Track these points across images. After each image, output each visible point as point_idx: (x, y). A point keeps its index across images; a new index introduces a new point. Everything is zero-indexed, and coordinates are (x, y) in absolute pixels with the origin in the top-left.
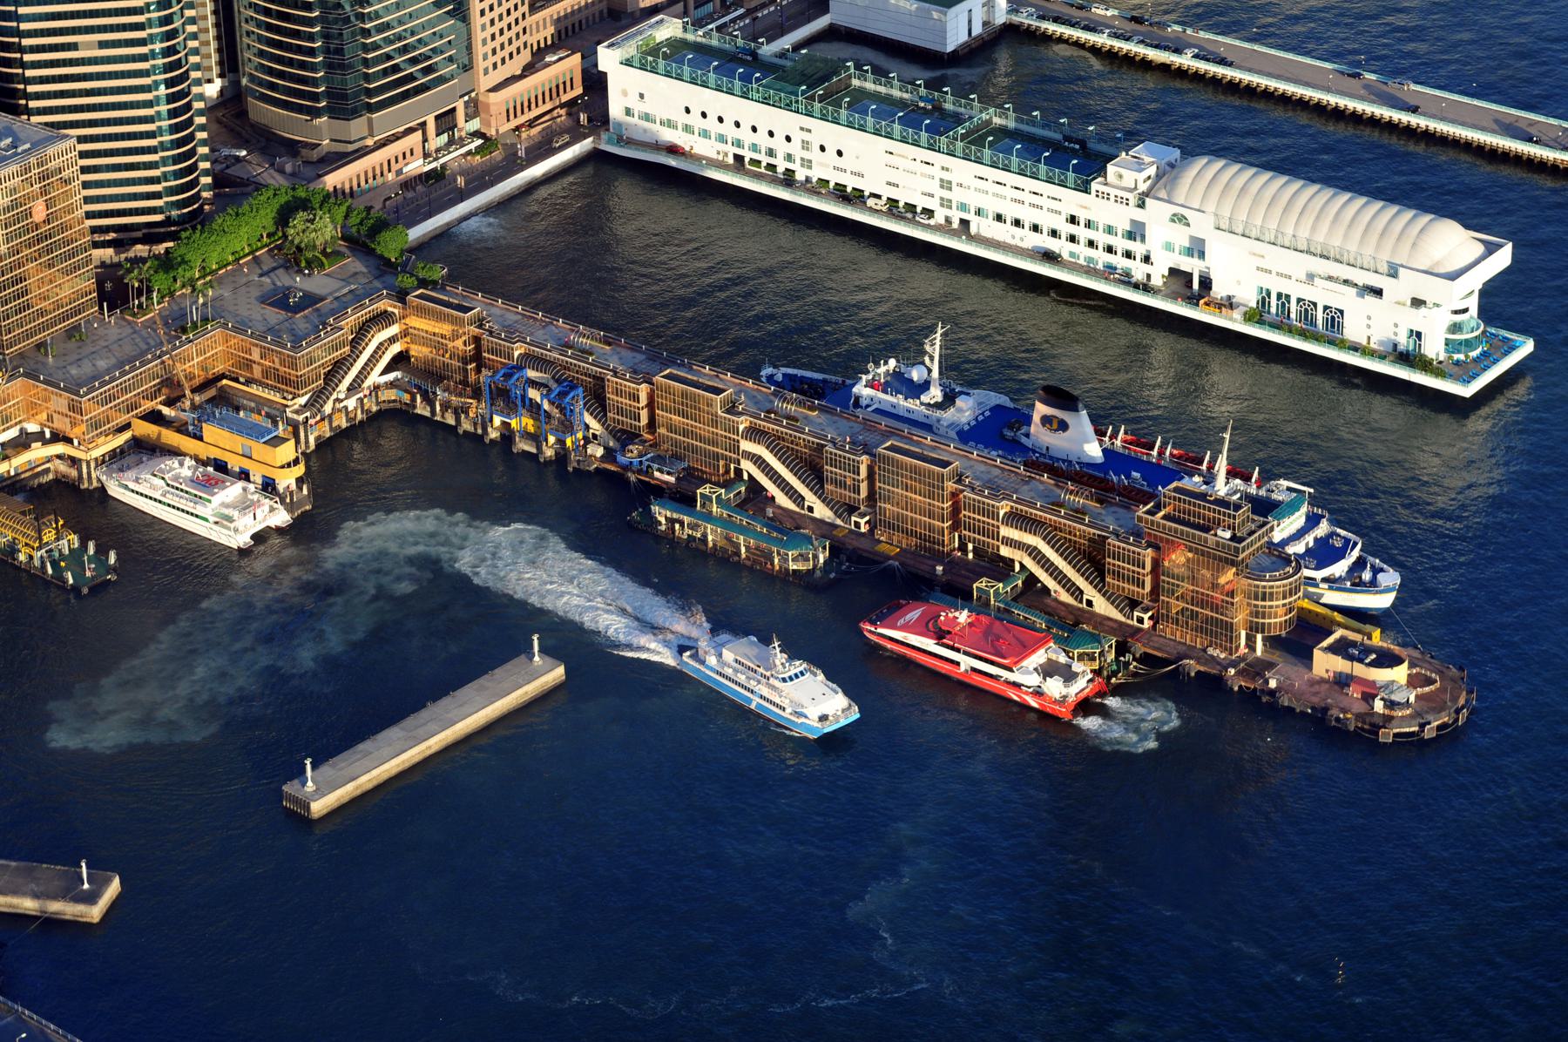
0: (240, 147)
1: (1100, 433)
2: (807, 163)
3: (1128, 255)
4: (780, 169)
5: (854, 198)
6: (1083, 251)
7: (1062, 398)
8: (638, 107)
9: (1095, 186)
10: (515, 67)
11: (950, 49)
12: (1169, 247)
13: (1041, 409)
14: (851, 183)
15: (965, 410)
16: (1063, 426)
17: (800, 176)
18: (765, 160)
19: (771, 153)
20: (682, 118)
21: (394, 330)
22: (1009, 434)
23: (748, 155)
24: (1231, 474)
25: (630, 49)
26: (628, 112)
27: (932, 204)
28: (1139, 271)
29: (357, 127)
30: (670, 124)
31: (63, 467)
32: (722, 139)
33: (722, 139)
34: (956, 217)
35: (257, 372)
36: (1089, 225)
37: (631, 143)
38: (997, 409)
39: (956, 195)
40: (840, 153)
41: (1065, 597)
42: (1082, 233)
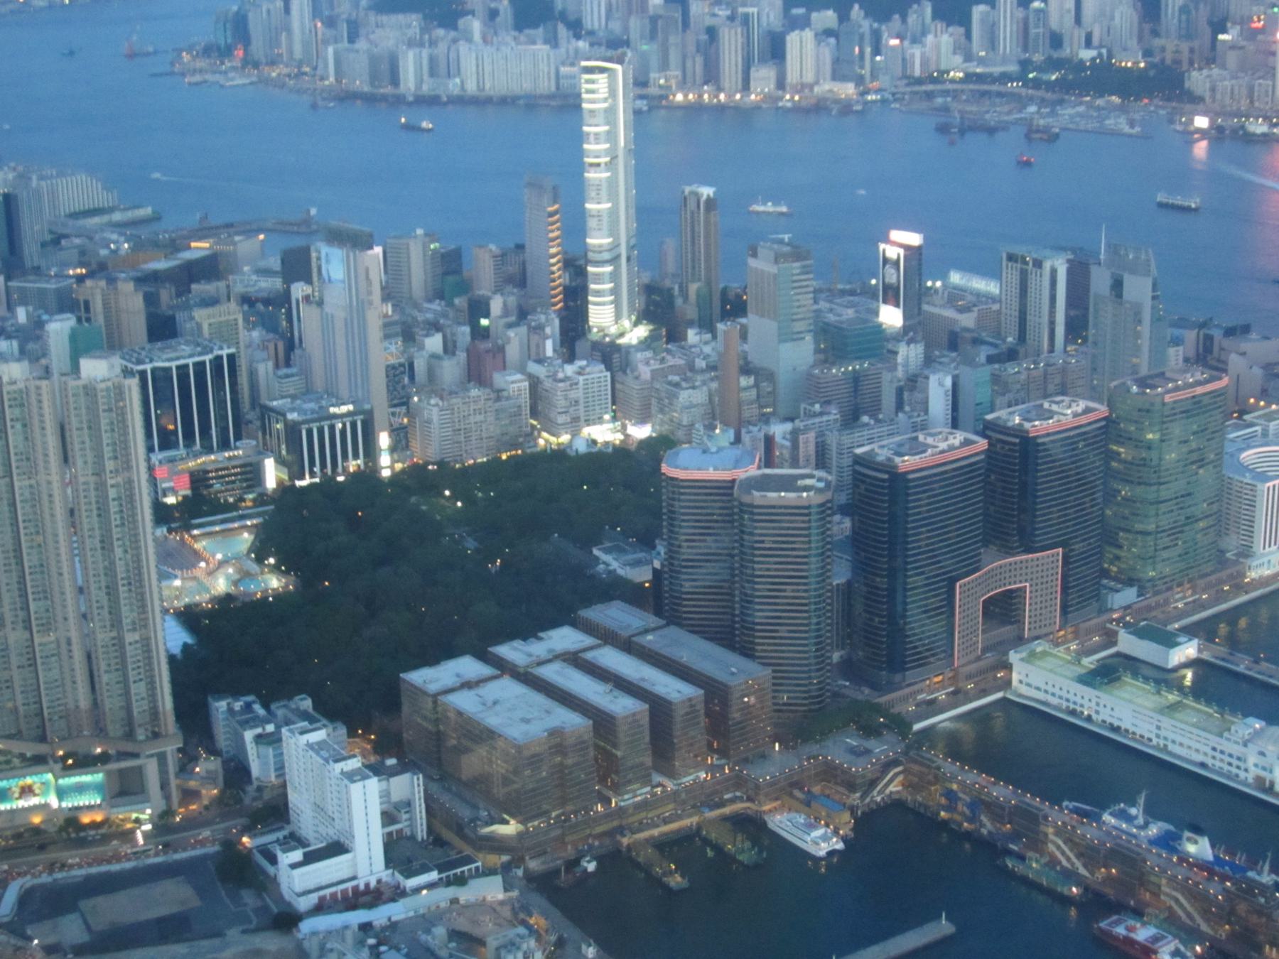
0: (847, 680)
1: (1213, 846)
2: (1097, 712)
3: (1238, 767)
4: (1086, 713)
5: (1116, 729)
6: (1218, 764)
7: (1198, 830)
8: (1025, 680)
9: (1226, 734)
10: (972, 657)
11: (1170, 666)
12: (1256, 765)
13: (1187, 834)
14: (1116, 723)
15: (1154, 830)
16: (1196, 842)
17: (1094, 717)
18: (1079, 709)
19: (1082, 706)
20: (1043, 687)
21: (900, 769)
22: (1171, 843)
23: (1072, 706)
24: (1269, 875)
25: (1024, 655)
26: (1021, 682)
27: (1153, 736)
28: (1242, 775)
29: (898, 677)
30: (1038, 689)
31: (749, 812)
32: (1060, 697)
33: (1060, 697)
34: (1162, 743)
35: (839, 781)
36: (1222, 752)
37: (1020, 696)
38: (1168, 833)
39: (1163, 733)
40: (1112, 709)
41: (1188, 922)
42: (1218, 755)
